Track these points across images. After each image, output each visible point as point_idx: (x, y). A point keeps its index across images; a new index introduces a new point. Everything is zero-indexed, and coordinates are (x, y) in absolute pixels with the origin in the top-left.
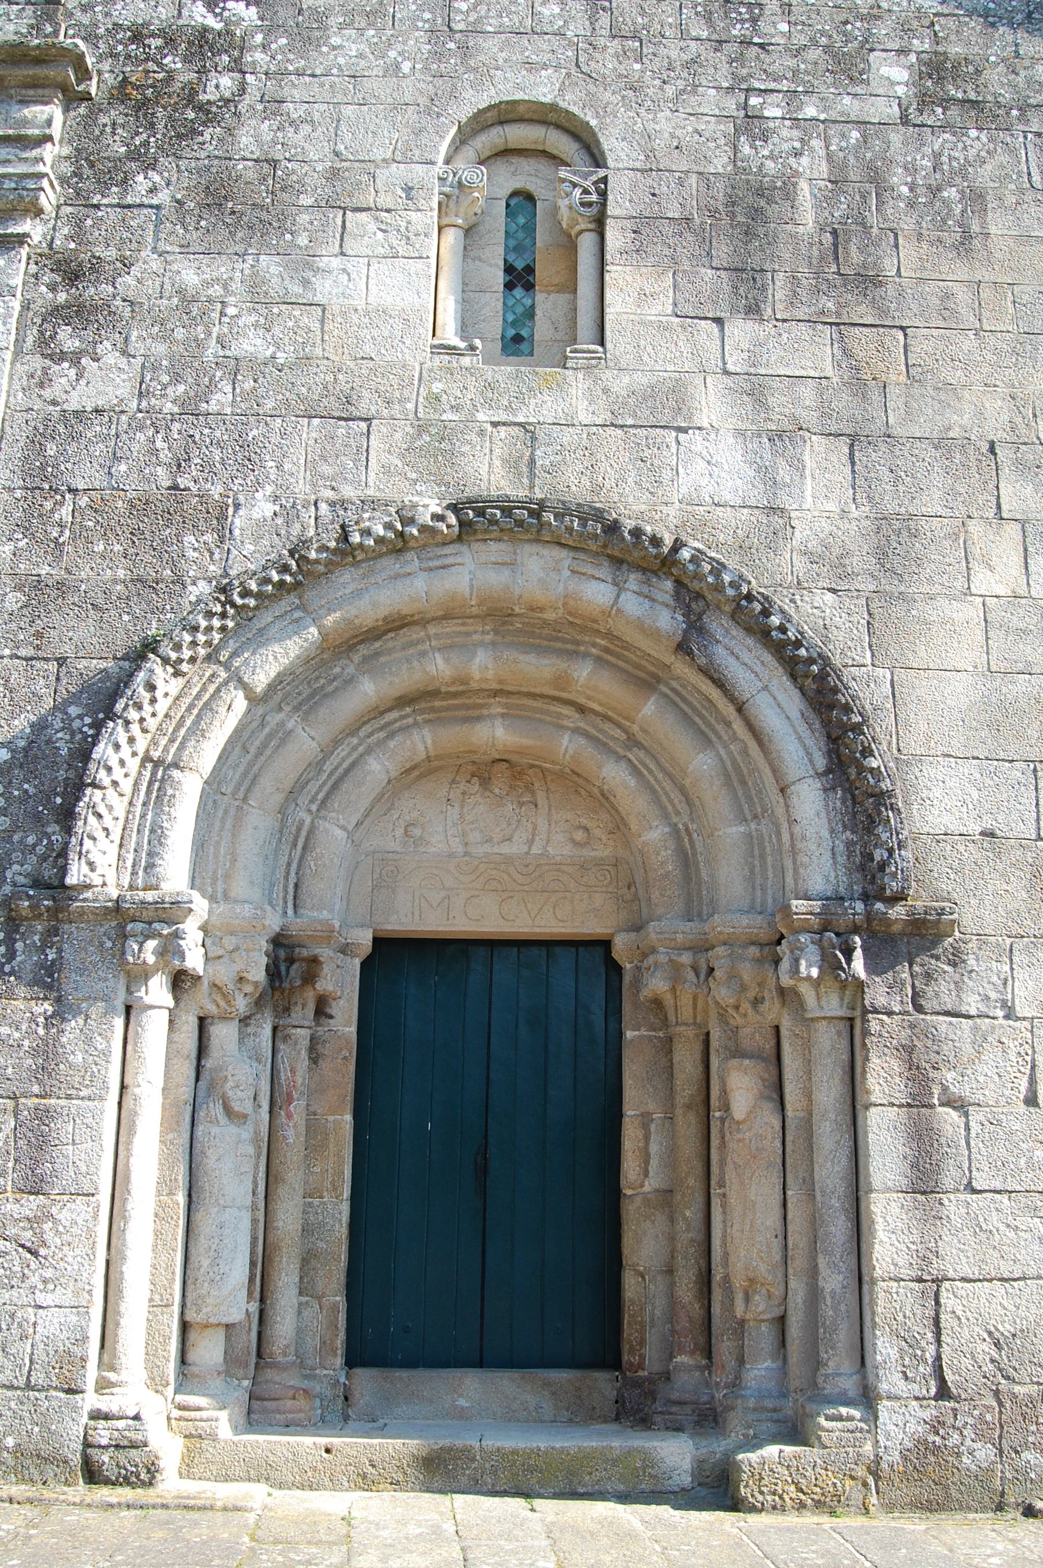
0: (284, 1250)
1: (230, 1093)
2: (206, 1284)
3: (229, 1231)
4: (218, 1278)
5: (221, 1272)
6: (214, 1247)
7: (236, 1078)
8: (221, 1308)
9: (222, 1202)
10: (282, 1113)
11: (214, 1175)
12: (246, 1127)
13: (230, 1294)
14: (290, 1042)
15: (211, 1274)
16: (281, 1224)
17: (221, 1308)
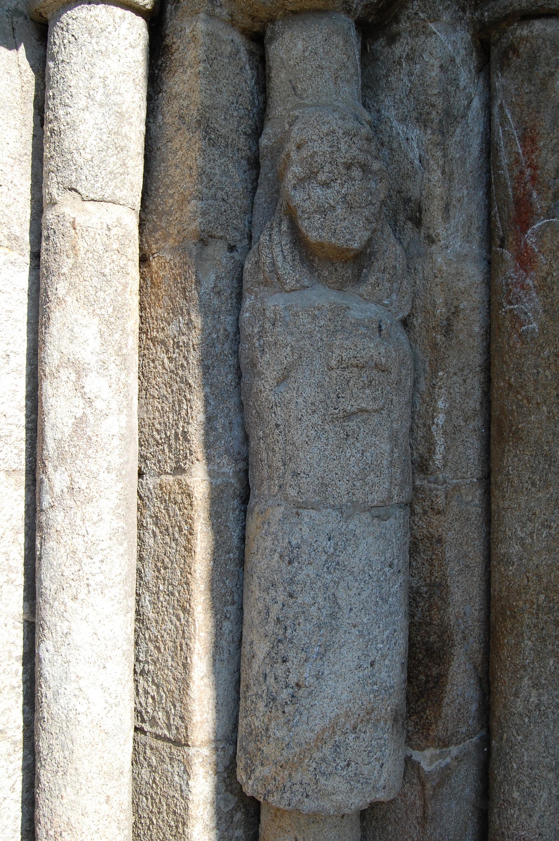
0: (527, 619)
1: (298, 197)
2: (261, 706)
3: (311, 571)
4: (285, 695)
5: (293, 679)
6: (275, 610)
7: (305, 153)
8: (297, 777)
9: (293, 492)
10: (508, 255)
11: (273, 419)
12: (364, 289)
13: (321, 740)
14: (515, 61)
15: (271, 680)
16: (516, 548)
17: (297, 777)
